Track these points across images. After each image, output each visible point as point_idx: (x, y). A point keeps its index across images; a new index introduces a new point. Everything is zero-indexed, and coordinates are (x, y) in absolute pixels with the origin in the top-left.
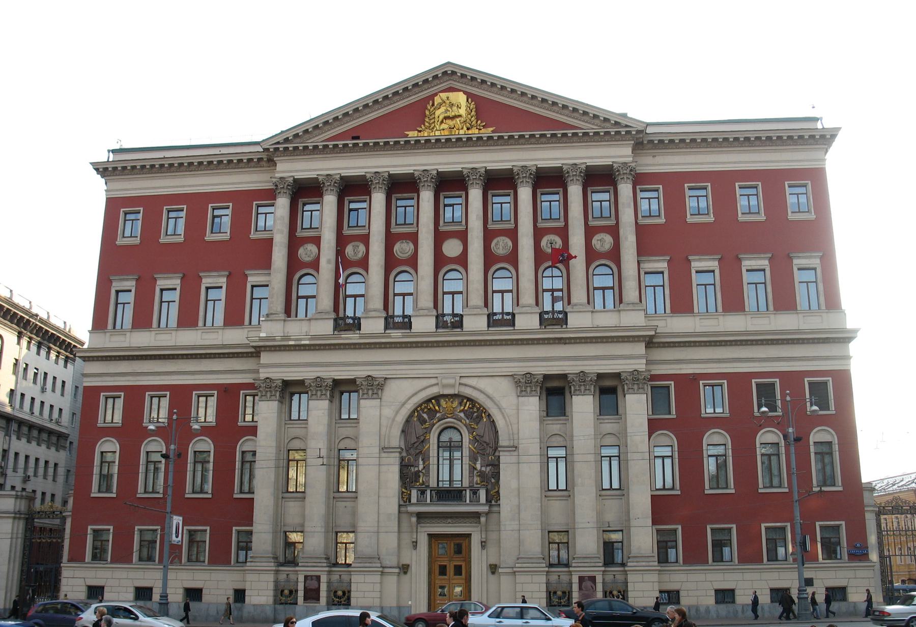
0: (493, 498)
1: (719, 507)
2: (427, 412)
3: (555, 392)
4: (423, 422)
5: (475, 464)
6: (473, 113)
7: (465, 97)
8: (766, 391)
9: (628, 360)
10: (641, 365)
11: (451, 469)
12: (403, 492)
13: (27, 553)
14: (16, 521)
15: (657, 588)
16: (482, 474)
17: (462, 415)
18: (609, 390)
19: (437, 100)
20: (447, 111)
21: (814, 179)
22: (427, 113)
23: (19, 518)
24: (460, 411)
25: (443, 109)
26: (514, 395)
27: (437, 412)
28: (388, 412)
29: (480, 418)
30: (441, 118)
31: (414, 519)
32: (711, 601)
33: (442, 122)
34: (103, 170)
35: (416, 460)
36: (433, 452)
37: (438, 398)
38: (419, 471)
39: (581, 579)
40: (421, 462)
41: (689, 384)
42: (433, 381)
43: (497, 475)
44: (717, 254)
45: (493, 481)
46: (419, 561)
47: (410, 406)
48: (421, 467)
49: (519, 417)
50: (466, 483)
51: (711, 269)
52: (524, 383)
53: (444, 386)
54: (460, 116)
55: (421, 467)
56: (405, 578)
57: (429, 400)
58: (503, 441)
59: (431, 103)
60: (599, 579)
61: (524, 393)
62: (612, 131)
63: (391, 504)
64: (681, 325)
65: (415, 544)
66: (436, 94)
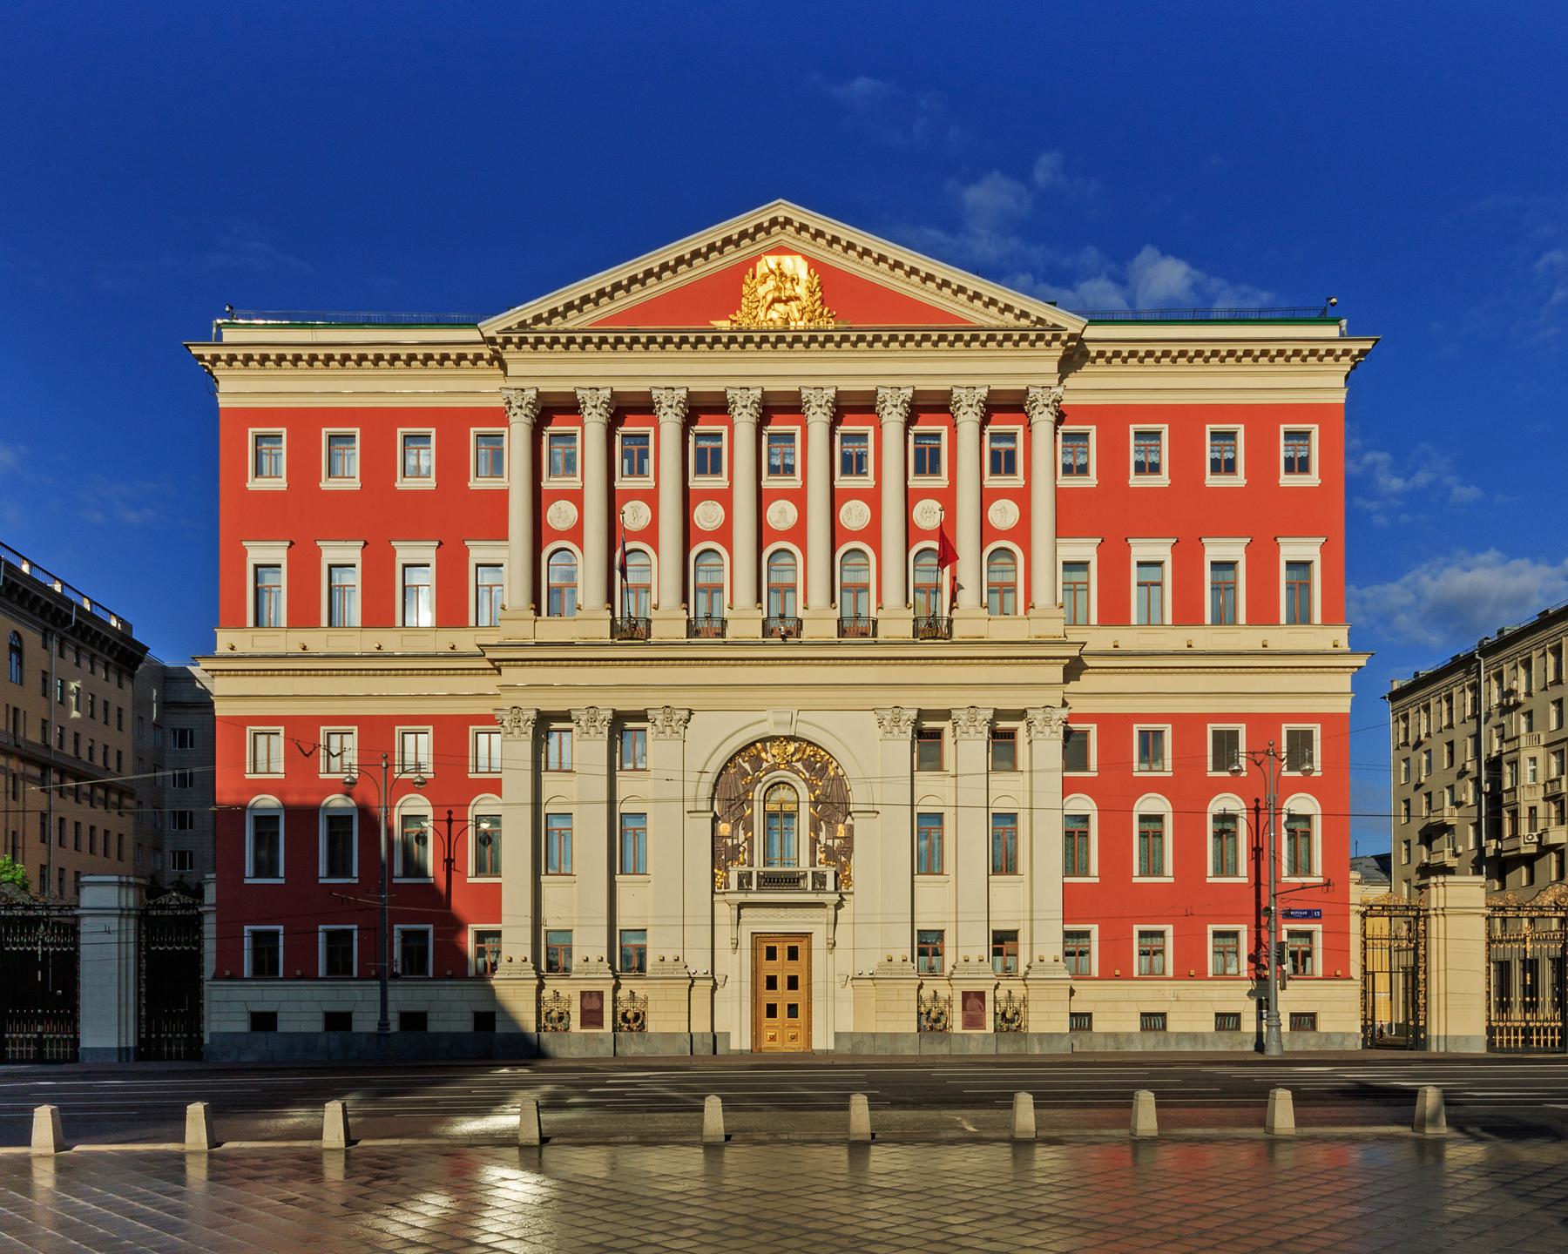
13: (143, 966)
14: (124, 921)
17: (799, 765)
19: (762, 268)
20: (778, 289)
22: (745, 290)
23: (128, 916)
25: (771, 283)
27: (762, 760)
30: (769, 298)
32: (1136, 1027)
33: (769, 308)
40: (741, 832)
52: (888, 723)
54: (797, 298)
55: (742, 837)
60: (989, 998)
66: (759, 258)
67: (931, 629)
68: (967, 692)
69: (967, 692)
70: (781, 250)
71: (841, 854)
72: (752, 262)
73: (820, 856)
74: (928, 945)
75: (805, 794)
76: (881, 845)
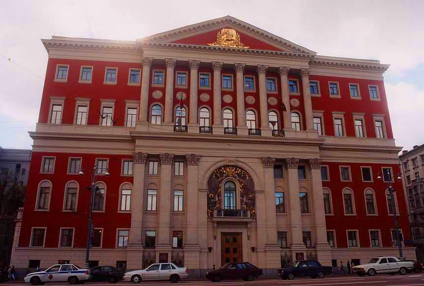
0: (254, 216)
1: (352, 222)
3: (280, 166)
4: (217, 177)
6: (239, 39)
7: (235, 32)
8: (366, 171)
9: (312, 154)
11: (229, 202)
12: (208, 212)
15: (331, 259)
16: (246, 204)
17: (236, 175)
18: (304, 166)
19: (223, 31)
20: (227, 37)
21: (380, 84)
24: (235, 174)
25: (225, 36)
26: (262, 167)
28: (202, 173)
30: (225, 39)
31: (216, 225)
35: (215, 195)
36: (223, 191)
37: (226, 166)
38: (216, 202)
39: (297, 254)
41: (334, 167)
42: (224, 158)
43: (254, 204)
44: (344, 111)
45: (252, 207)
47: (212, 169)
48: (217, 199)
49: (263, 177)
50: (239, 207)
51: (341, 118)
52: (266, 162)
53: (229, 161)
54: (233, 40)
55: (217, 199)
56: (211, 254)
57: (220, 168)
58: (257, 188)
59: (219, 32)
60: (305, 254)
62: (302, 54)
63: (204, 217)
64: (329, 141)
65: (215, 238)
66: (222, 29)
71: (252, 204)
72: (220, 30)
74: (282, 235)
75: (238, 186)
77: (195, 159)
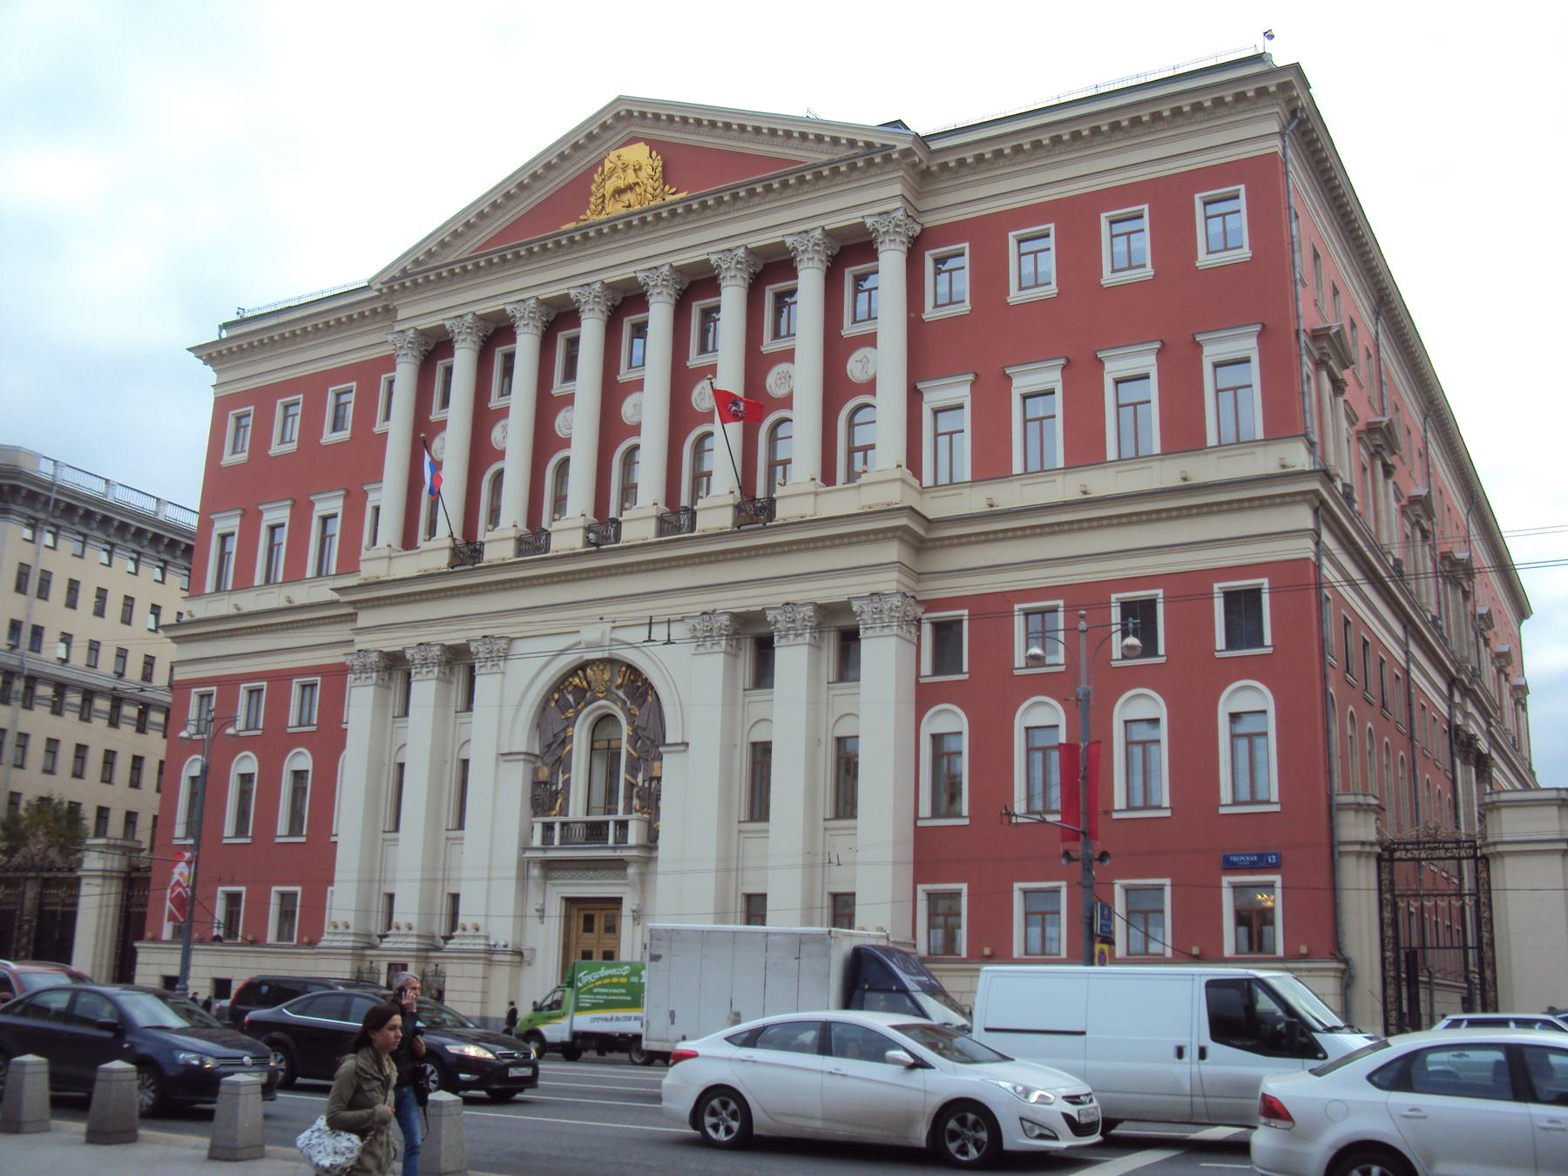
2: (568, 690)
3: (756, 643)
5: (635, 777)
9: (870, 577)
10: (889, 582)
29: (644, 696)
34: (209, 354)
37: (583, 666)
46: (546, 939)
53: (591, 646)
57: (573, 672)
61: (701, 649)
65: (542, 913)
67: (754, 510)
68: (781, 587)
69: (781, 587)
70: (633, 140)
73: (636, 802)
76: (694, 787)
77: (502, 652)
